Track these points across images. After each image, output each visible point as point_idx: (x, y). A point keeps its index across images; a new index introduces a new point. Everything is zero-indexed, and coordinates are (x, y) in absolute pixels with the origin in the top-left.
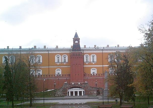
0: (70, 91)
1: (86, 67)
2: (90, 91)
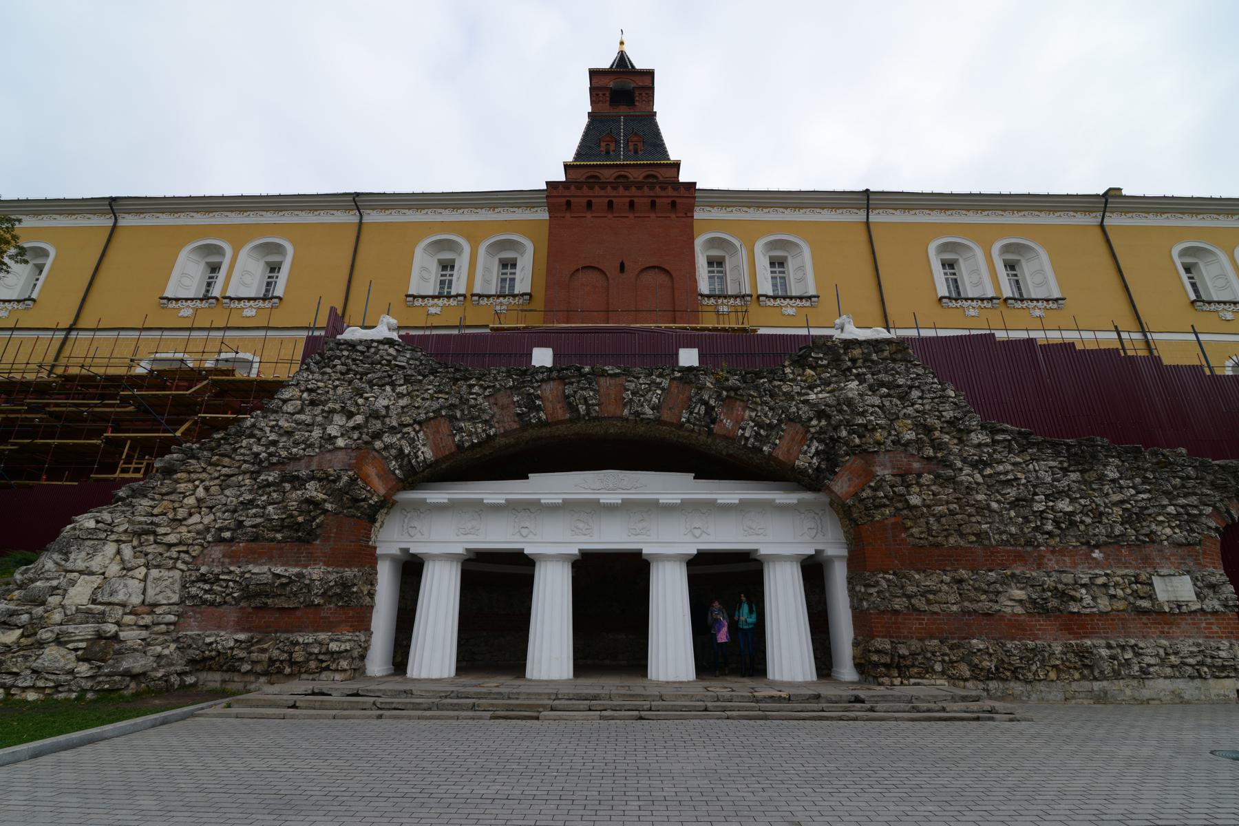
0: (444, 532)
2: (1023, 549)
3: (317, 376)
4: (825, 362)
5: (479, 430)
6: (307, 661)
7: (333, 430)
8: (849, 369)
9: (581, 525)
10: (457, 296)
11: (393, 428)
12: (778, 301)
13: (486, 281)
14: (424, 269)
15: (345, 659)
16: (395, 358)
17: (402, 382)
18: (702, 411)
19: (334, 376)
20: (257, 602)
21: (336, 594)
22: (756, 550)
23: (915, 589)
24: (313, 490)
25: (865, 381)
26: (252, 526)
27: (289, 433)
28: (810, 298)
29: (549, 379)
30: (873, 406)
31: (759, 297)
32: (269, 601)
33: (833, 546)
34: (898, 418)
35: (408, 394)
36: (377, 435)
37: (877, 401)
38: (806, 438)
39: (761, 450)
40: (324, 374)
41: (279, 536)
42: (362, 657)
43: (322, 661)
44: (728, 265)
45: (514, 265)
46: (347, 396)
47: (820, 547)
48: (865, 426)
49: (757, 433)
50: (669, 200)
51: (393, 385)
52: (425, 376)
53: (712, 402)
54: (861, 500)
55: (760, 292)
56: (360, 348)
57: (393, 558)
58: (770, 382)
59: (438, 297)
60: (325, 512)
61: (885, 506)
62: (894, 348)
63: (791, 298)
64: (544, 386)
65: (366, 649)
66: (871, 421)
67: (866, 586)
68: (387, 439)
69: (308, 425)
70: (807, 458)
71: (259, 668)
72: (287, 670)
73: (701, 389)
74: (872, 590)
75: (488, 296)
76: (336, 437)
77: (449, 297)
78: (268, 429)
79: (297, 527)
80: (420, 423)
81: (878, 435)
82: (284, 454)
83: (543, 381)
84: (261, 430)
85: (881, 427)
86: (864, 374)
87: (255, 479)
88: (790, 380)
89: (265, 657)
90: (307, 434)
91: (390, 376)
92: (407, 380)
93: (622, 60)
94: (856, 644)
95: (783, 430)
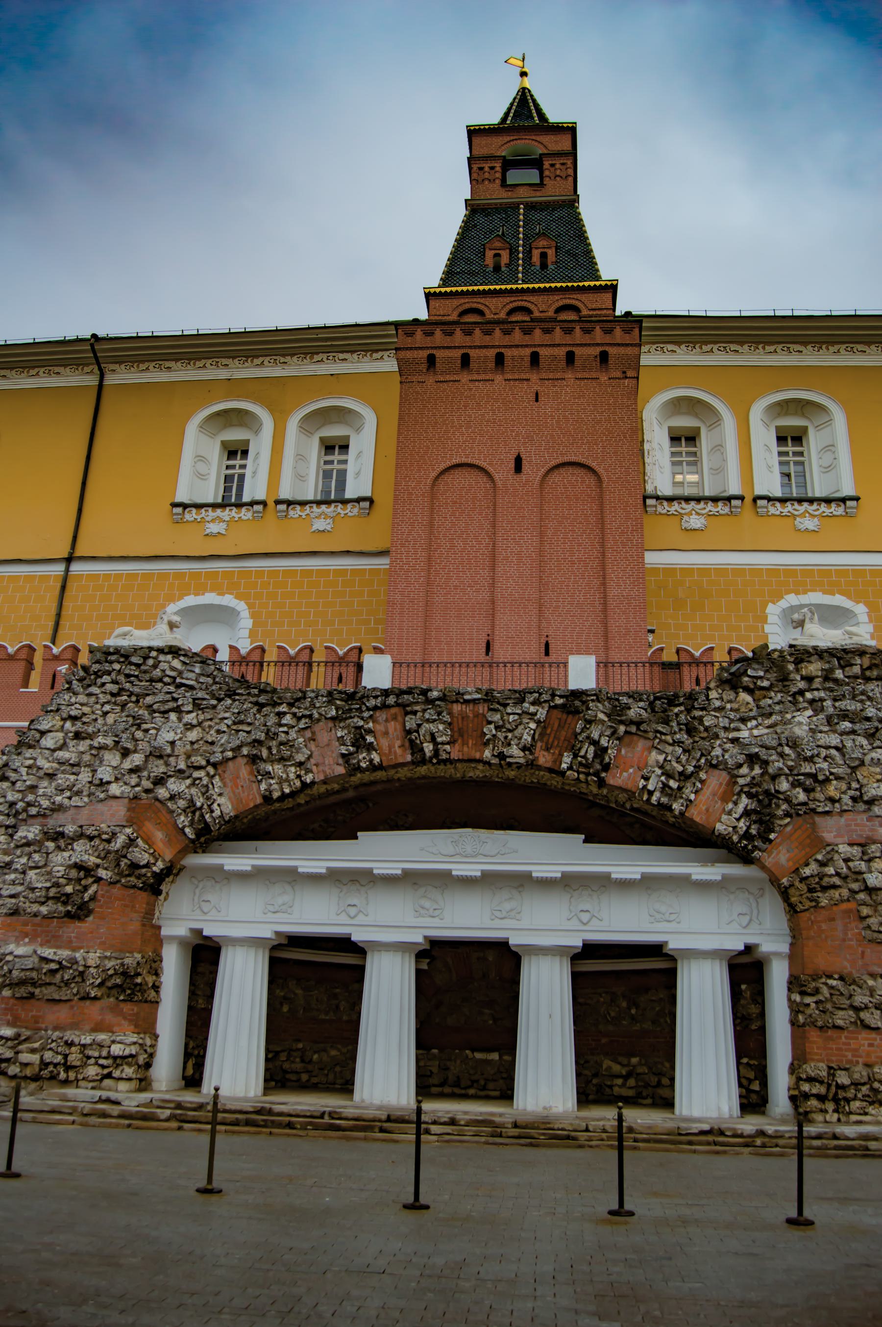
0: (248, 907)
1: (670, 571)
3: (82, 698)
4: (766, 684)
5: (292, 776)
6: (85, 1065)
7: (105, 774)
8: (801, 692)
9: (427, 904)
10: (252, 504)
11: (181, 771)
12: (789, 507)
13: (300, 477)
14: (200, 458)
15: (130, 1065)
16: (180, 673)
17: (190, 708)
18: (590, 756)
19: (103, 698)
20: (22, 991)
21: (116, 986)
22: (666, 942)
23: (866, 1000)
24: (82, 852)
25: (822, 709)
26: (12, 896)
27: (51, 776)
28: (844, 500)
29: (385, 706)
30: (827, 747)
31: (755, 499)
32: (37, 991)
33: (772, 940)
34: (862, 763)
35: (200, 724)
36: (160, 781)
37: (834, 740)
38: (729, 794)
39: (669, 808)
40: (90, 695)
41: (44, 910)
42: (148, 1065)
43: (103, 1067)
44: (705, 441)
45: (344, 448)
46: (122, 726)
47: (751, 940)
48: (814, 776)
49: (665, 786)
50: (598, 350)
51: (178, 710)
52: (220, 700)
53: (604, 742)
54: (803, 879)
55: (758, 491)
56: (134, 659)
57: (182, 942)
58: (688, 711)
59: (222, 506)
60: (99, 880)
61: (835, 887)
62: (866, 662)
63: (811, 501)
64: (378, 714)
65: (151, 1056)
66: (821, 769)
67: (803, 993)
68: (174, 785)
69: (73, 765)
70: (729, 821)
71: (28, 1072)
72: (62, 1075)
73: (590, 722)
74: (808, 1000)
75: (302, 503)
76: (109, 783)
77: (239, 505)
78: (24, 771)
79: (66, 899)
80: (215, 765)
81: (832, 790)
82: (45, 803)
83: (375, 708)
84: (15, 770)
85: (838, 778)
86: (822, 700)
87: (11, 836)
88: (715, 710)
89: (35, 1058)
90: (72, 778)
91: (175, 700)
92: (197, 705)
93: (524, 102)
94: (792, 1069)
95: (702, 782)
